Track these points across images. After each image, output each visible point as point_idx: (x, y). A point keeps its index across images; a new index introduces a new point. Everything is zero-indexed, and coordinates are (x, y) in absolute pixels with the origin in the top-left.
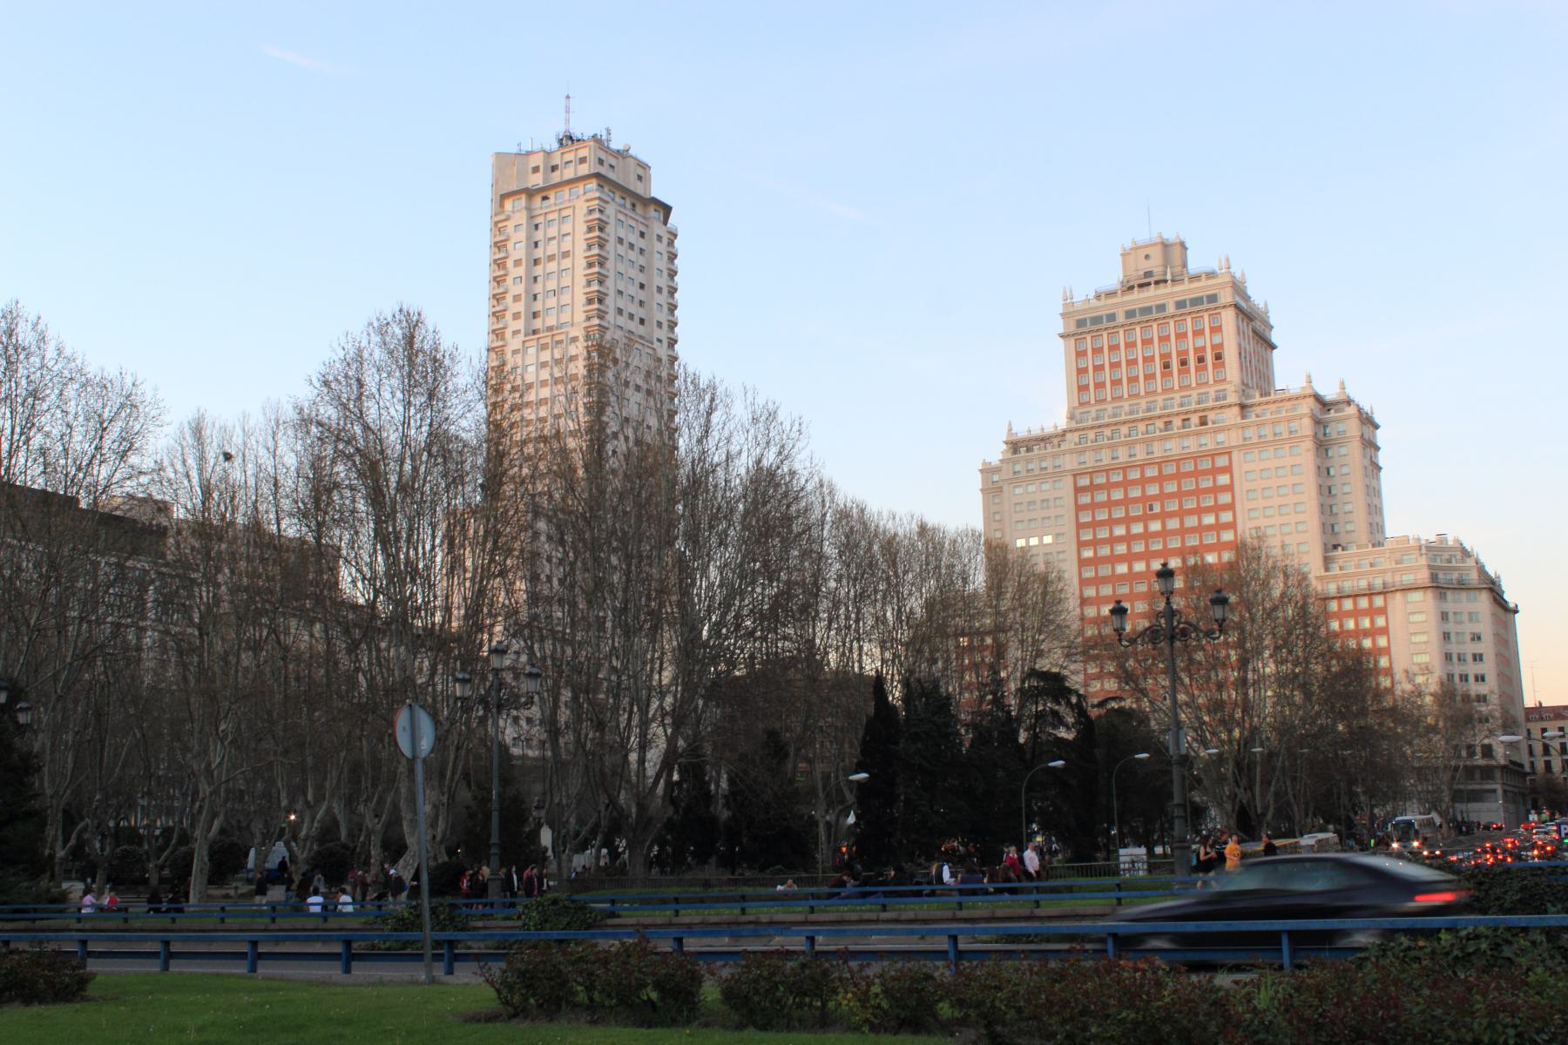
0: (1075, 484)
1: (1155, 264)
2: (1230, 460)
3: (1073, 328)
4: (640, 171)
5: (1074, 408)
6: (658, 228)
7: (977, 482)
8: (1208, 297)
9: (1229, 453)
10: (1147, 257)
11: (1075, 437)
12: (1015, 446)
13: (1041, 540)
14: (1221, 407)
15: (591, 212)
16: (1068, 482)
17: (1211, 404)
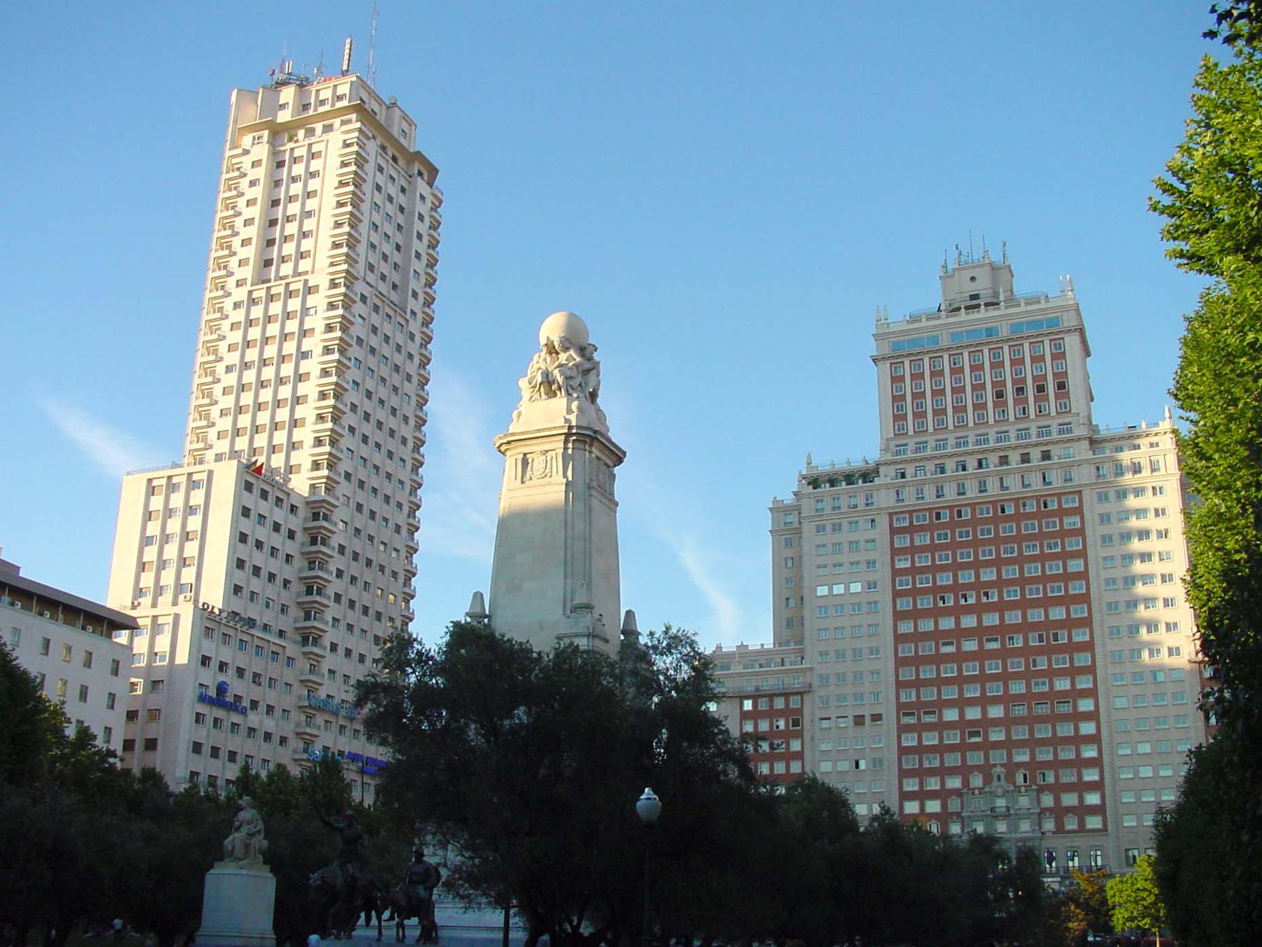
0: (891, 525)
1: (982, 286)
2: (1081, 501)
3: (887, 351)
4: (405, 126)
5: (888, 439)
6: (422, 186)
7: (767, 522)
8: (1047, 320)
9: (1080, 492)
10: (973, 279)
11: (892, 469)
12: (815, 482)
13: (847, 588)
14: (1068, 441)
15: (346, 145)
16: (883, 521)
17: (1055, 436)
